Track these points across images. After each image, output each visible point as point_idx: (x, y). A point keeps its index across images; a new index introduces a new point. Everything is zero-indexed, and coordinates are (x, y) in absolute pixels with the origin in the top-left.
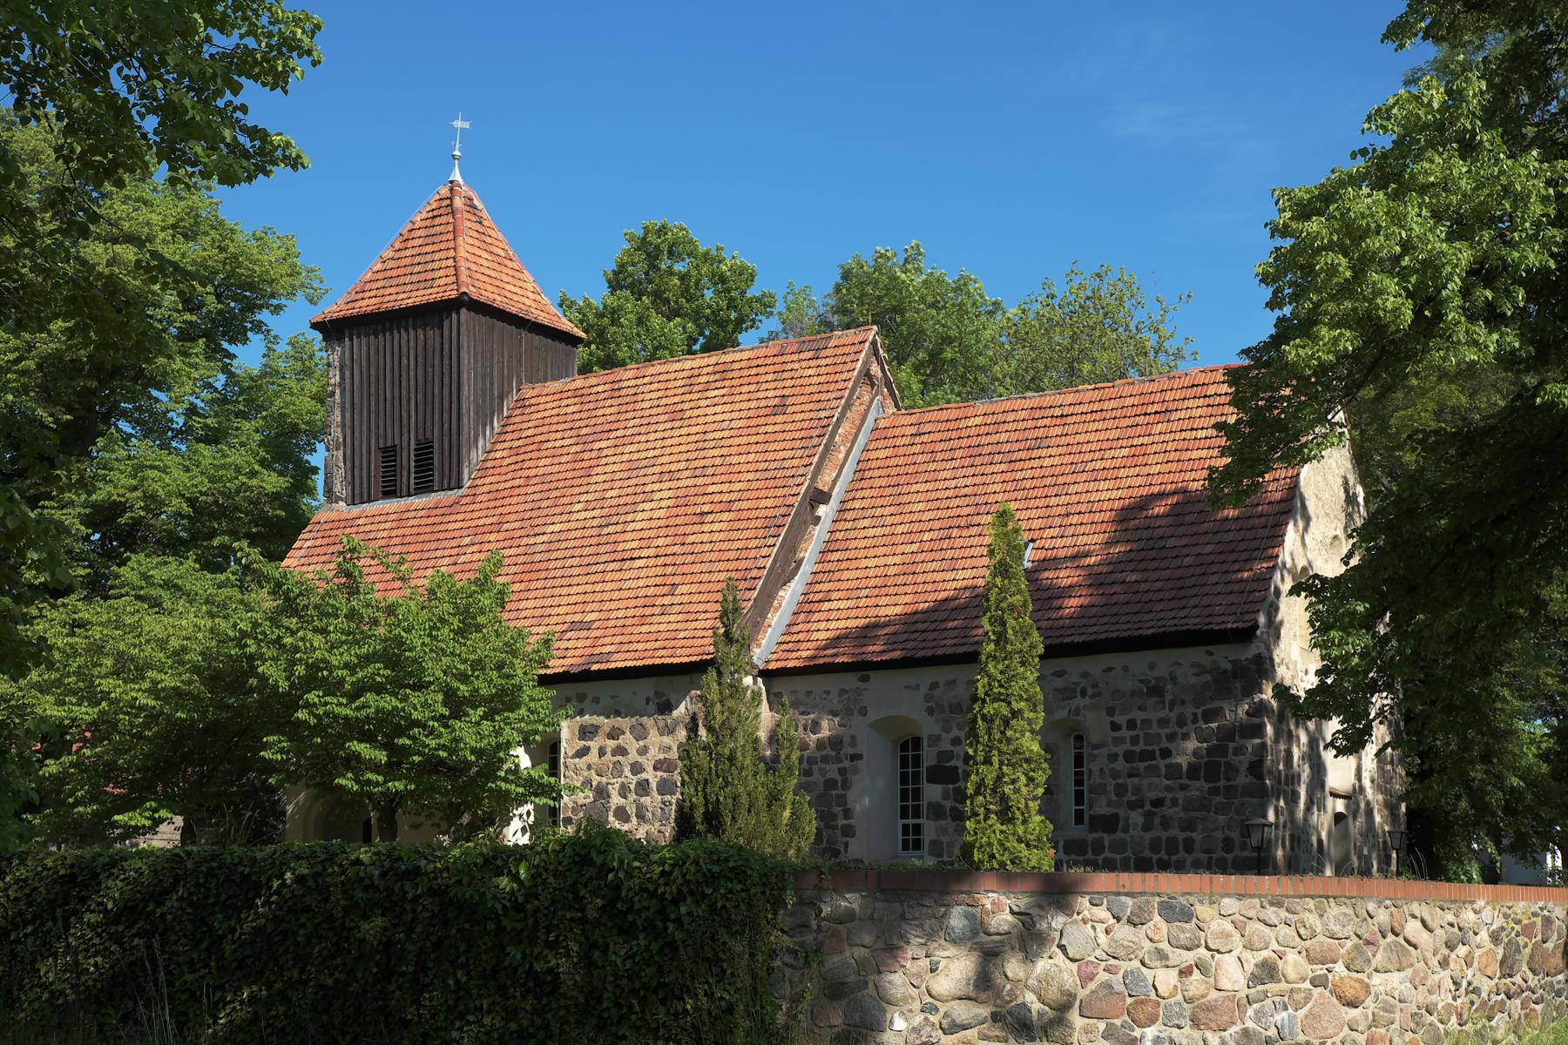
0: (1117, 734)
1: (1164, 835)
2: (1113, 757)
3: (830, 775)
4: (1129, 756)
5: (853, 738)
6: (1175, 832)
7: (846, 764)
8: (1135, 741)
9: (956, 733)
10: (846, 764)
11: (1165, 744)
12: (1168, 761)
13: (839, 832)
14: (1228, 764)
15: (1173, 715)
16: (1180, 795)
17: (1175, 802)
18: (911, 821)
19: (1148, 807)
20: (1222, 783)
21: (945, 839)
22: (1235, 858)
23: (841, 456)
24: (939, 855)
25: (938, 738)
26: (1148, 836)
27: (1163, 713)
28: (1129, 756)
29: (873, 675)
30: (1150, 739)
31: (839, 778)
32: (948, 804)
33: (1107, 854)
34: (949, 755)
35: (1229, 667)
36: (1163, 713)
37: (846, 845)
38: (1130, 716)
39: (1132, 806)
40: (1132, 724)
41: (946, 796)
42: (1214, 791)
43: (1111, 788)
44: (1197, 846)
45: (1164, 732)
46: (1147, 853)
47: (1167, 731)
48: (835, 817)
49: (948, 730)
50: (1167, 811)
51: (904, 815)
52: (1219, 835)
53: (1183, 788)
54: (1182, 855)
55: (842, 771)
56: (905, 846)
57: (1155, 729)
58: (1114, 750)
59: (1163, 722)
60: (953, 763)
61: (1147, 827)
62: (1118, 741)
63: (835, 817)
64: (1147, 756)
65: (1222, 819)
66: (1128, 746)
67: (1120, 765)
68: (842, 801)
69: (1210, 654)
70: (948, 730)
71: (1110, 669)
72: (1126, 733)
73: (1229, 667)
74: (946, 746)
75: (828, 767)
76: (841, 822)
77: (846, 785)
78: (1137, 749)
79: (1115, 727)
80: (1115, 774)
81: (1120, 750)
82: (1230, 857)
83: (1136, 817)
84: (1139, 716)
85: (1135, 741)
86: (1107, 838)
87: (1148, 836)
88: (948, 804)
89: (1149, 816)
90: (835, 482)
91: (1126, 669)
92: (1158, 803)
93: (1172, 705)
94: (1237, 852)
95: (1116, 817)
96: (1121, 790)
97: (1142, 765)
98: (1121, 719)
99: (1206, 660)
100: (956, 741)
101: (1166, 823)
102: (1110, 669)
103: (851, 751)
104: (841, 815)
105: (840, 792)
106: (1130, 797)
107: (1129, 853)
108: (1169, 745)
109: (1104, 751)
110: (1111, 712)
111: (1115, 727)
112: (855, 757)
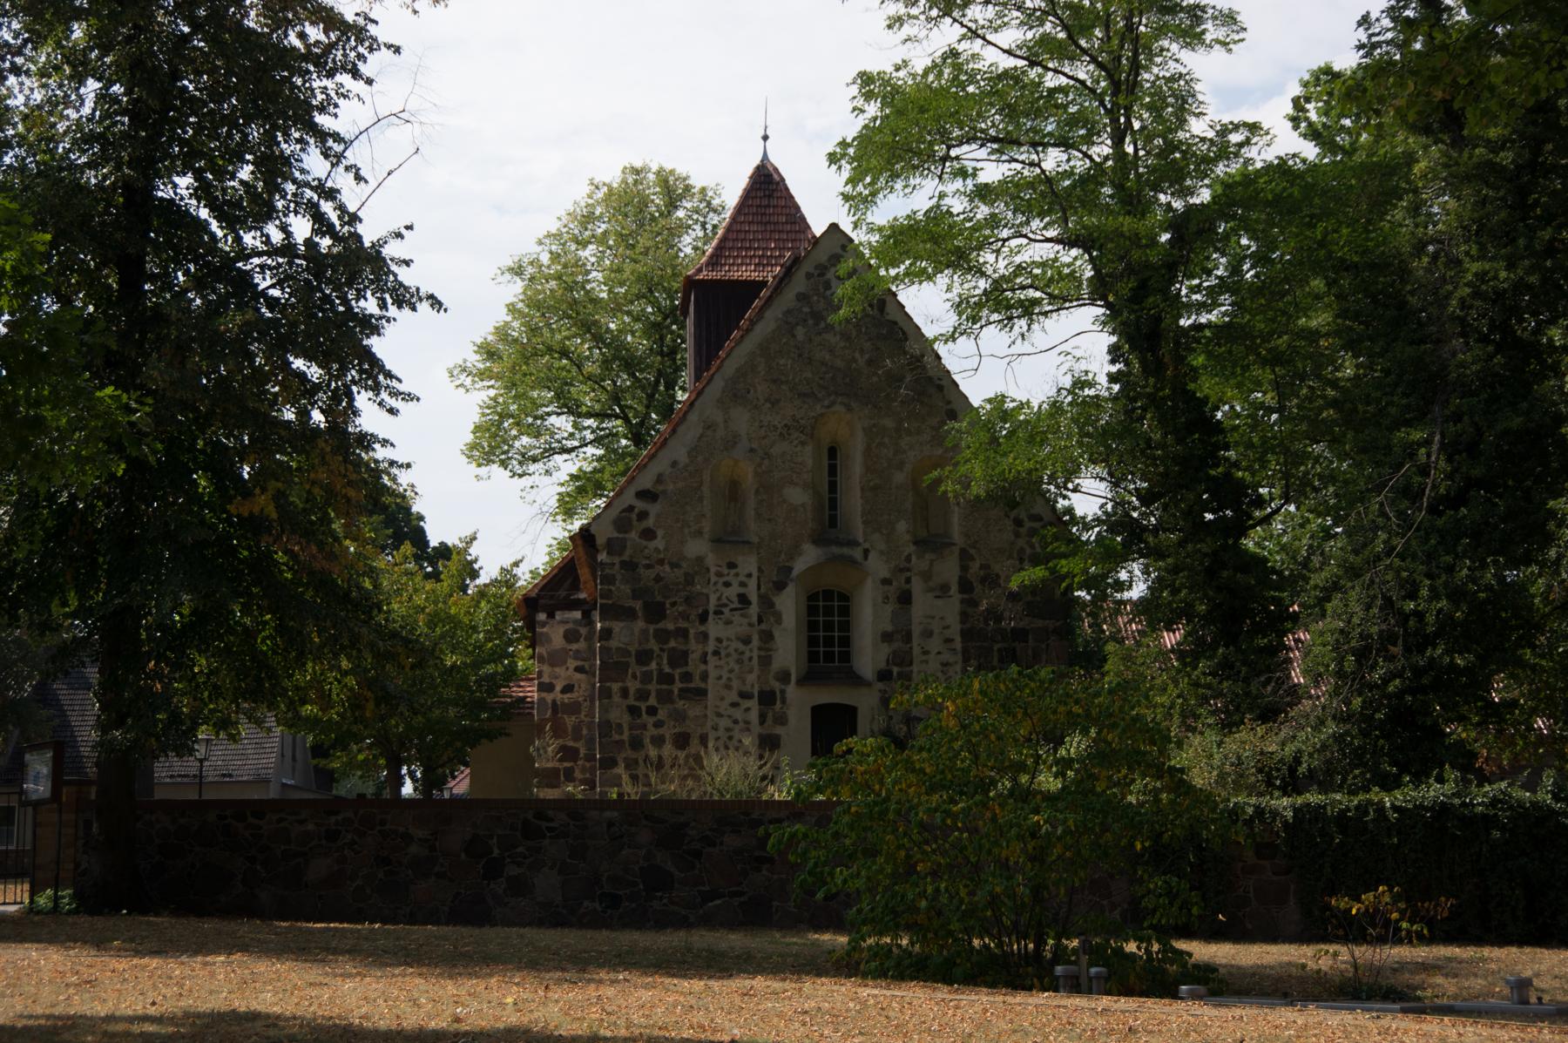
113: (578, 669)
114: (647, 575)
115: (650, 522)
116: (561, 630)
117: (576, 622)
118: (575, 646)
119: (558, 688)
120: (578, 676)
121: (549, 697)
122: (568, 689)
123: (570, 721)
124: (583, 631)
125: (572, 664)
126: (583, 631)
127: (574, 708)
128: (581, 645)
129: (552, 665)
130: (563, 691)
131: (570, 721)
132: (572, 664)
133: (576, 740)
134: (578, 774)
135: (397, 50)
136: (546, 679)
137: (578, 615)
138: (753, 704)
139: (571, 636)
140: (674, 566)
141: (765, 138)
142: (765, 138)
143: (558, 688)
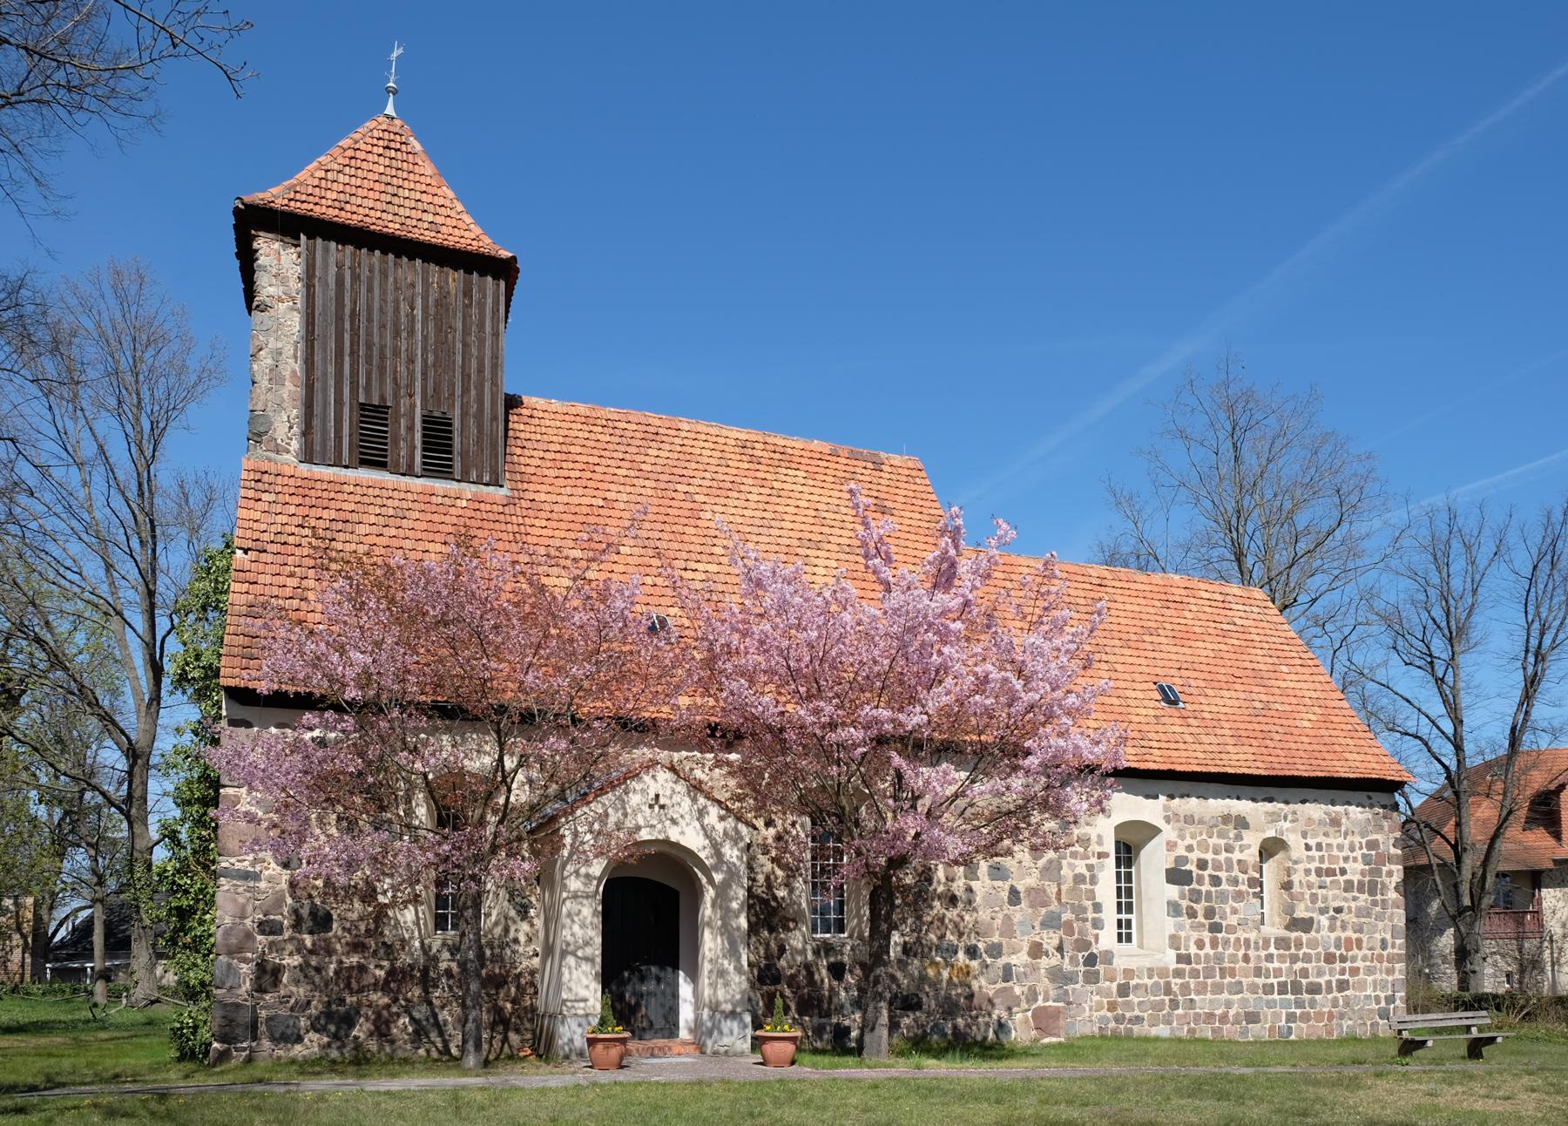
1: (1343, 935)
2: (1307, 872)
3: (1078, 870)
4: (1319, 872)
5: (1099, 836)
6: (1349, 933)
7: (1094, 861)
8: (1322, 859)
9: (1188, 841)
10: (1094, 861)
11: (1342, 864)
13: (1089, 925)
15: (1347, 842)
16: (1353, 905)
17: (1350, 911)
18: (1124, 916)
19: (1332, 913)
20: (1379, 897)
21: (1183, 934)
24: (1178, 948)
25: (1175, 844)
26: (1333, 936)
27: (1340, 840)
28: (1319, 872)
30: (1333, 859)
31: (1088, 874)
32: (1185, 903)
33: (1305, 950)
34: (1185, 860)
36: (1340, 840)
37: (1097, 937)
38: (1318, 840)
39: (1323, 911)
40: (1319, 847)
41: (1182, 897)
42: (1375, 903)
43: (1307, 897)
46: (1332, 950)
48: (1085, 910)
49: (1182, 838)
50: (1343, 916)
51: (1120, 911)
52: (1378, 936)
53: (1355, 899)
54: (1355, 951)
55: (1090, 868)
56: (1120, 940)
57: (1335, 852)
59: (1340, 847)
60: (1188, 867)
61: (1332, 929)
63: (1085, 910)
64: (1330, 872)
65: (1381, 925)
66: (1317, 864)
67: (1313, 878)
68: (1091, 895)
70: (1182, 838)
72: (1314, 853)
74: (1184, 853)
75: (1077, 862)
77: (1093, 880)
79: (1308, 848)
80: (1310, 886)
81: (1313, 866)
83: (1324, 921)
84: (1325, 841)
85: (1322, 859)
86: (1304, 937)
87: (1333, 936)
88: (1185, 903)
89: (1333, 919)
92: (1338, 910)
93: (1346, 834)
94: (1389, 950)
95: (1311, 919)
96: (1314, 898)
97: (1329, 879)
98: (1312, 842)
100: (1190, 848)
101: (1344, 928)
103: (1099, 849)
104: (1090, 908)
105: (1089, 887)
106: (1320, 904)
107: (1320, 949)
108: (1346, 866)
109: (1301, 867)
110: (1304, 835)
111: (1308, 848)
112: (1101, 855)
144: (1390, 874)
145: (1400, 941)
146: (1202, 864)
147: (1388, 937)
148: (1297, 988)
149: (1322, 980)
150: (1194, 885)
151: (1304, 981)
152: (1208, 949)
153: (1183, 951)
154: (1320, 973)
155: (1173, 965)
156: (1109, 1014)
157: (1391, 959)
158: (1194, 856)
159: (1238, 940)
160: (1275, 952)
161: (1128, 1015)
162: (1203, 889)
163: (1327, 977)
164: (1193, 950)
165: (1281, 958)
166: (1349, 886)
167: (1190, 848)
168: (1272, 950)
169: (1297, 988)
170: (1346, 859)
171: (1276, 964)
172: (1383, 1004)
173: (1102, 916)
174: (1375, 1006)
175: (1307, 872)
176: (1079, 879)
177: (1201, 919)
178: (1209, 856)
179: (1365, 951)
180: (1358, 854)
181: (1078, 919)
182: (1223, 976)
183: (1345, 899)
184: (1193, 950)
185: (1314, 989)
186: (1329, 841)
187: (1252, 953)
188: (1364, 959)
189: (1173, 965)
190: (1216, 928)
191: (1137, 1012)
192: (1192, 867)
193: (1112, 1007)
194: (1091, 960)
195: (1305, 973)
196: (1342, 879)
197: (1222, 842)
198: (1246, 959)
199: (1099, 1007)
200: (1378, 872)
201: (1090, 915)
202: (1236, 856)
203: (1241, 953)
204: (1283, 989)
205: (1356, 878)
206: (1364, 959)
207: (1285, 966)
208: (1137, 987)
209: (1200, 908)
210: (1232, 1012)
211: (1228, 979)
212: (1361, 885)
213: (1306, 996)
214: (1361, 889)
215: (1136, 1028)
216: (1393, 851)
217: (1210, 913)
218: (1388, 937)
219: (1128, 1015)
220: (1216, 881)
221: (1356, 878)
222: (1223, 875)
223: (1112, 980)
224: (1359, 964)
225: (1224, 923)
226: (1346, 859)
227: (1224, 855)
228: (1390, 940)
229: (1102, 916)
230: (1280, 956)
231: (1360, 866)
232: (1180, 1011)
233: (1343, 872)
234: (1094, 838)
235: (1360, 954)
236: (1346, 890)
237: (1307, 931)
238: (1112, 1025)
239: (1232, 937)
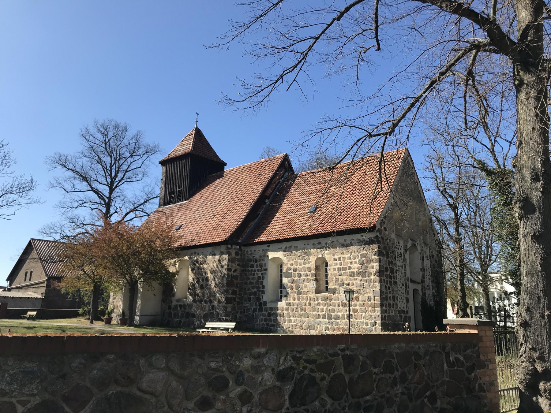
0: (336, 262)
2: (334, 269)
4: (340, 270)
7: (263, 272)
8: (341, 264)
9: (291, 262)
11: (349, 265)
12: (350, 271)
14: (368, 272)
16: (354, 282)
19: (345, 286)
20: (367, 278)
22: (371, 304)
23: (274, 187)
25: (287, 264)
29: (271, 245)
33: (333, 301)
35: (368, 240)
38: (339, 256)
40: (340, 259)
43: (334, 279)
44: (360, 299)
45: (349, 261)
47: (350, 261)
49: (289, 261)
55: (262, 274)
58: (335, 267)
60: (291, 271)
62: (337, 264)
64: (345, 269)
66: (339, 266)
67: (336, 272)
68: (262, 283)
69: (362, 236)
71: (333, 241)
72: (338, 262)
73: (368, 240)
74: (289, 266)
76: (261, 289)
77: (263, 278)
78: (341, 267)
81: (336, 267)
82: (370, 303)
84: (342, 256)
86: (333, 296)
88: (289, 284)
90: (271, 193)
91: (337, 241)
93: (351, 252)
94: (372, 301)
95: (335, 289)
97: (343, 272)
99: (361, 238)
100: (292, 265)
102: (333, 241)
106: (339, 282)
108: (351, 266)
111: (335, 260)
113: (238, 265)
114: (386, 242)
115: (385, 226)
116: (235, 251)
117: (238, 249)
118: (237, 257)
119: (233, 270)
120: (238, 267)
121: (230, 273)
122: (235, 271)
123: (235, 281)
124: (240, 252)
125: (237, 263)
126: (240, 252)
127: (236, 277)
128: (239, 257)
129: (232, 263)
130: (234, 272)
131: (235, 281)
132: (237, 263)
133: (237, 288)
134: (237, 300)
135: (379, 49)
136: (230, 267)
137: (238, 247)
138: (404, 287)
139: (237, 254)
140: (390, 241)
141: (197, 122)
142: (197, 122)
143: (233, 270)
144: (373, 267)
145: (378, 298)
146: (295, 270)
147: (371, 295)
148: (330, 317)
149: (340, 314)
150: (293, 278)
151: (333, 314)
152: (297, 301)
153: (288, 301)
154: (339, 311)
155: (285, 307)
156: (265, 323)
157: (374, 306)
158: (292, 267)
159: (307, 297)
160: (321, 302)
161: (270, 323)
162: (295, 279)
163: (343, 313)
164: (292, 301)
165: (324, 305)
166: (352, 274)
167: (292, 265)
168: (320, 301)
169: (330, 317)
170: (351, 263)
171: (321, 307)
172: (369, 326)
173: (264, 290)
174: (365, 326)
175: (334, 269)
176: (259, 278)
177: (294, 290)
178: (297, 267)
179: (360, 302)
180: (357, 260)
181: (258, 291)
182: (301, 311)
183: (351, 280)
184: (292, 301)
185: (337, 318)
186: (344, 256)
187: (311, 302)
188: (360, 305)
189: (285, 307)
190: (299, 293)
191: (273, 323)
192: (292, 271)
193: (266, 320)
194: (261, 304)
195: (333, 311)
196: (348, 271)
197: (302, 261)
198: (310, 304)
199: (262, 320)
200: (366, 268)
201: (261, 289)
202: (307, 265)
203: (307, 302)
204: (324, 318)
205: (355, 271)
206: (360, 305)
207: (325, 308)
208: (273, 313)
209: (294, 285)
210: (304, 325)
211: (303, 312)
212: (359, 274)
213: (333, 320)
214: (359, 274)
215: (272, 328)
216: (374, 257)
217: (298, 287)
218: (371, 295)
219: (270, 323)
220: (300, 275)
221: (355, 271)
222: (302, 273)
223: (266, 311)
224: (358, 307)
225: (302, 291)
226: (351, 263)
227: (303, 265)
228: (372, 297)
229: (264, 290)
230: (323, 304)
231: (358, 265)
232: (286, 323)
233: (350, 268)
234: (263, 264)
235: (358, 303)
236: (351, 276)
237: (334, 294)
238: (266, 326)
239: (305, 296)
